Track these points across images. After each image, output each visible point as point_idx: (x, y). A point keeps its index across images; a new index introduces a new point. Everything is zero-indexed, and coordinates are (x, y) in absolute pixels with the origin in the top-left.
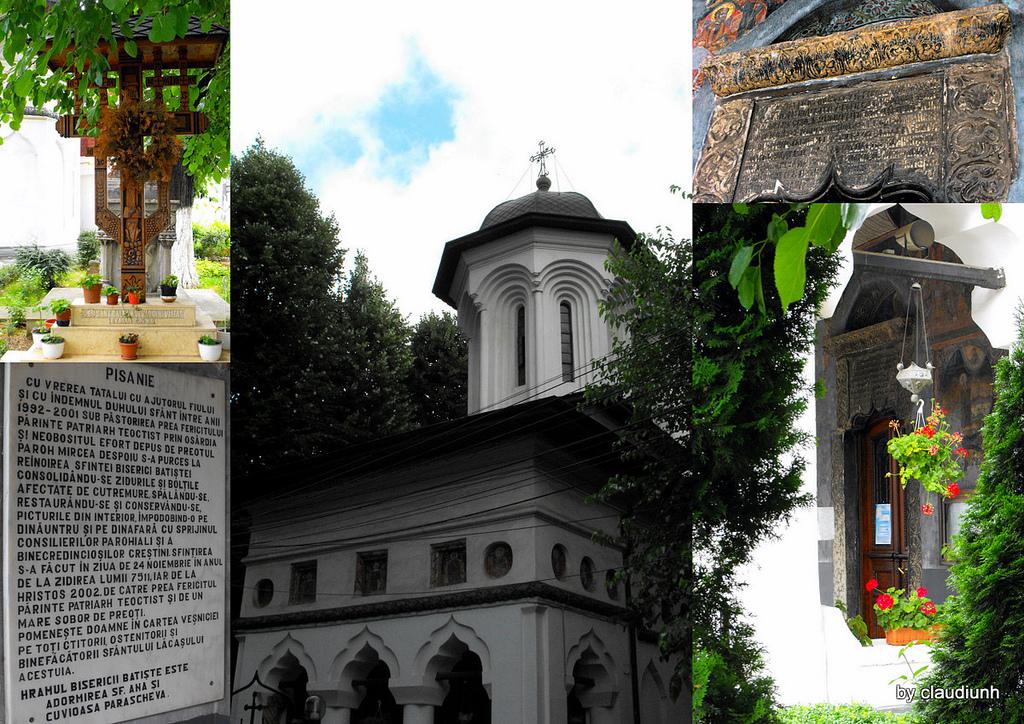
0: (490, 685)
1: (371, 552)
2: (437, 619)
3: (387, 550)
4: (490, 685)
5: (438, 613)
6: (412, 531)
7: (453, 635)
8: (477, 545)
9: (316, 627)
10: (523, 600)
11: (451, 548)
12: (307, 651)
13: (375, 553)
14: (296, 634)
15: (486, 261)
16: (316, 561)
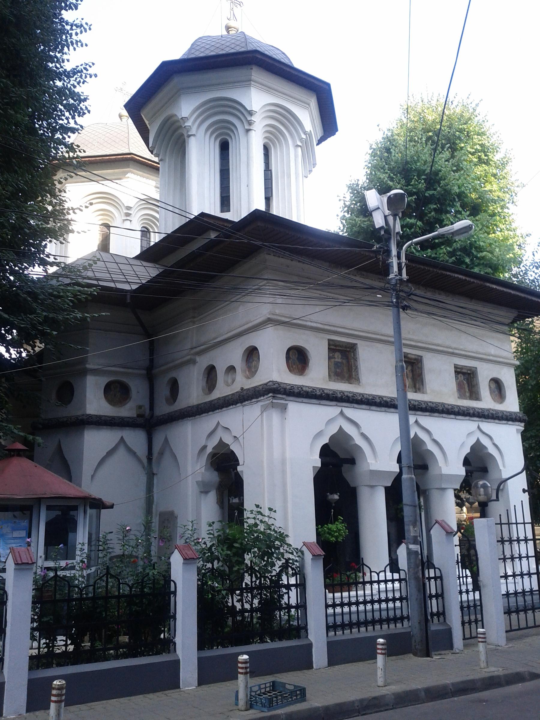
0: (242, 471)
1: (408, 354)
2: (330, 411)
3: (422, 357)
4: (242, 471)
5: (469, 420)
6: (370, 335)
7: (478, 439)
8: (485, 373)
9: (507, 424)
10: (517, 423)
11: (464, 371)
12: (363, 430)
13: (409, 356)
14: (351, 412)
15: (269, 89)
16: (355, 345)
